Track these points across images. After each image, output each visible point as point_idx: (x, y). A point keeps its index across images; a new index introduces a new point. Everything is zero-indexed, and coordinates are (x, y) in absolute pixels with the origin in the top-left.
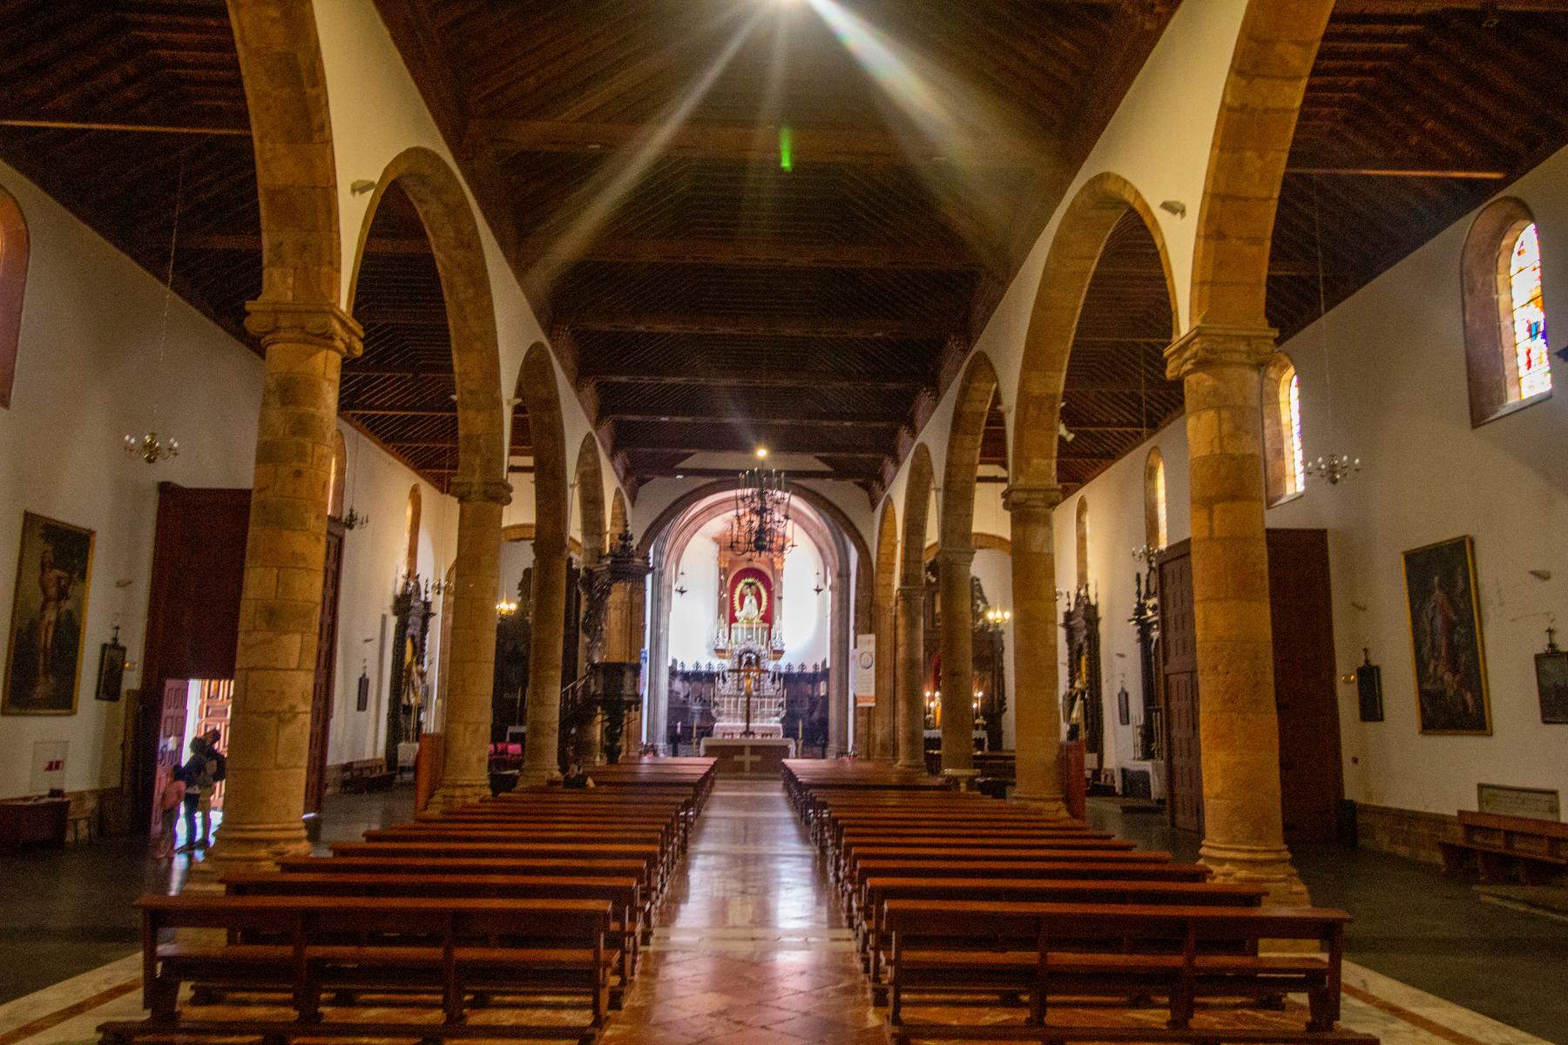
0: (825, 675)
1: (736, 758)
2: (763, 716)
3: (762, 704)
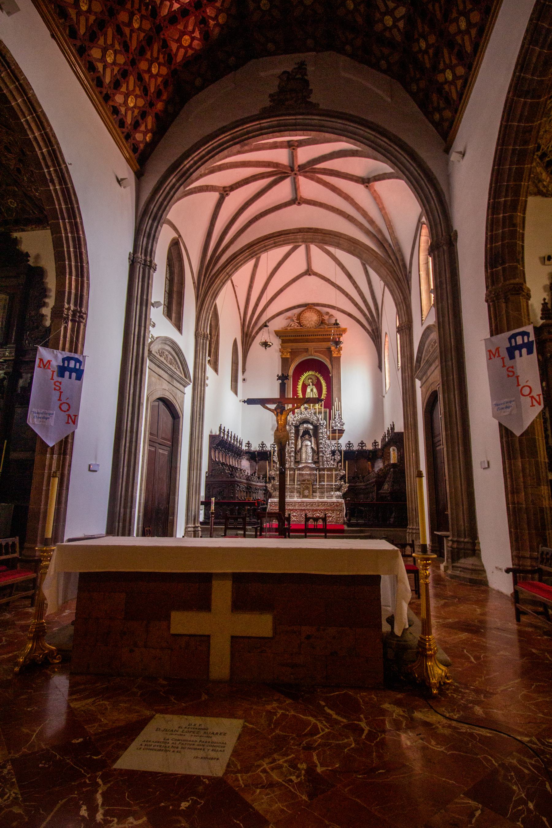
0: (395, 439)
1: (183, 623)
3: (321, 477)
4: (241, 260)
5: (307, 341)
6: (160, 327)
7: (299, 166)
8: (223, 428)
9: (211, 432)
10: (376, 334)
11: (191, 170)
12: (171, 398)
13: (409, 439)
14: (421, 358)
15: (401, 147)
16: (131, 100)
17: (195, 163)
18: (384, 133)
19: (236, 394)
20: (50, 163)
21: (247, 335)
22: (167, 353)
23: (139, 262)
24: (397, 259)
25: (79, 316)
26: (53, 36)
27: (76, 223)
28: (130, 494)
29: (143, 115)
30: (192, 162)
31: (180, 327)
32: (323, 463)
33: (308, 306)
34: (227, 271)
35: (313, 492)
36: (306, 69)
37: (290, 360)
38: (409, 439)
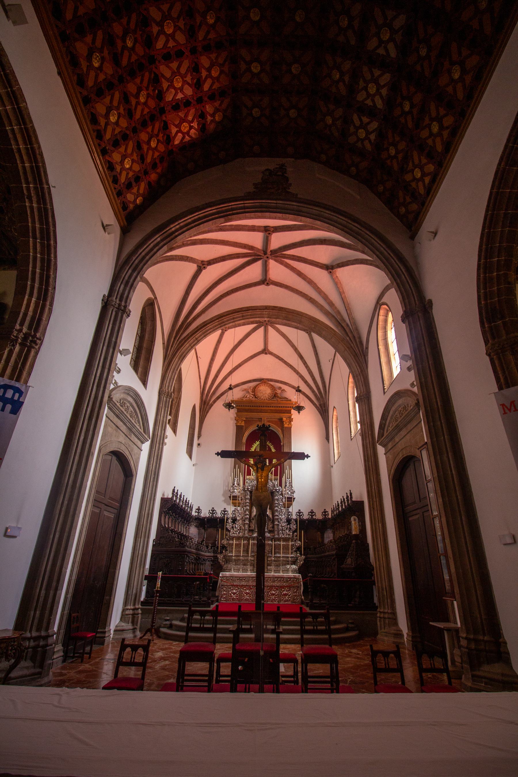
0: (352, 508)
2: (278, 564)
3: (277, 547)
4: (211, 329)
5: (261, 411)
6: (124, 375)
7: (271, 251)
8: (176, 491)
9: (163, 495)
10: (324, 408)
11: (177, 234)
12: (127, 453)
13: (373, 509)
14: (385, 424)
15: (372, 232)
16: (128, 162)
17: (181, 228)
18: (355, 220)
19: (191, 457)
20: (30, 179)
21: (205, 402)
22: (129, 405)
23: (112, 305)
24: (354, 337)
25: (31, 341)
26: (59, 73)
27: (49, 245)
28: (57, 569)
29: (137, 179)
30: (178, 227)
31: (145, 381)
32: (278, 532)
33: (262, 381)
34: (196, 337)
35: (268, 566)
36: (286, 169)
37: (244, 428)
38: (373, 509)
